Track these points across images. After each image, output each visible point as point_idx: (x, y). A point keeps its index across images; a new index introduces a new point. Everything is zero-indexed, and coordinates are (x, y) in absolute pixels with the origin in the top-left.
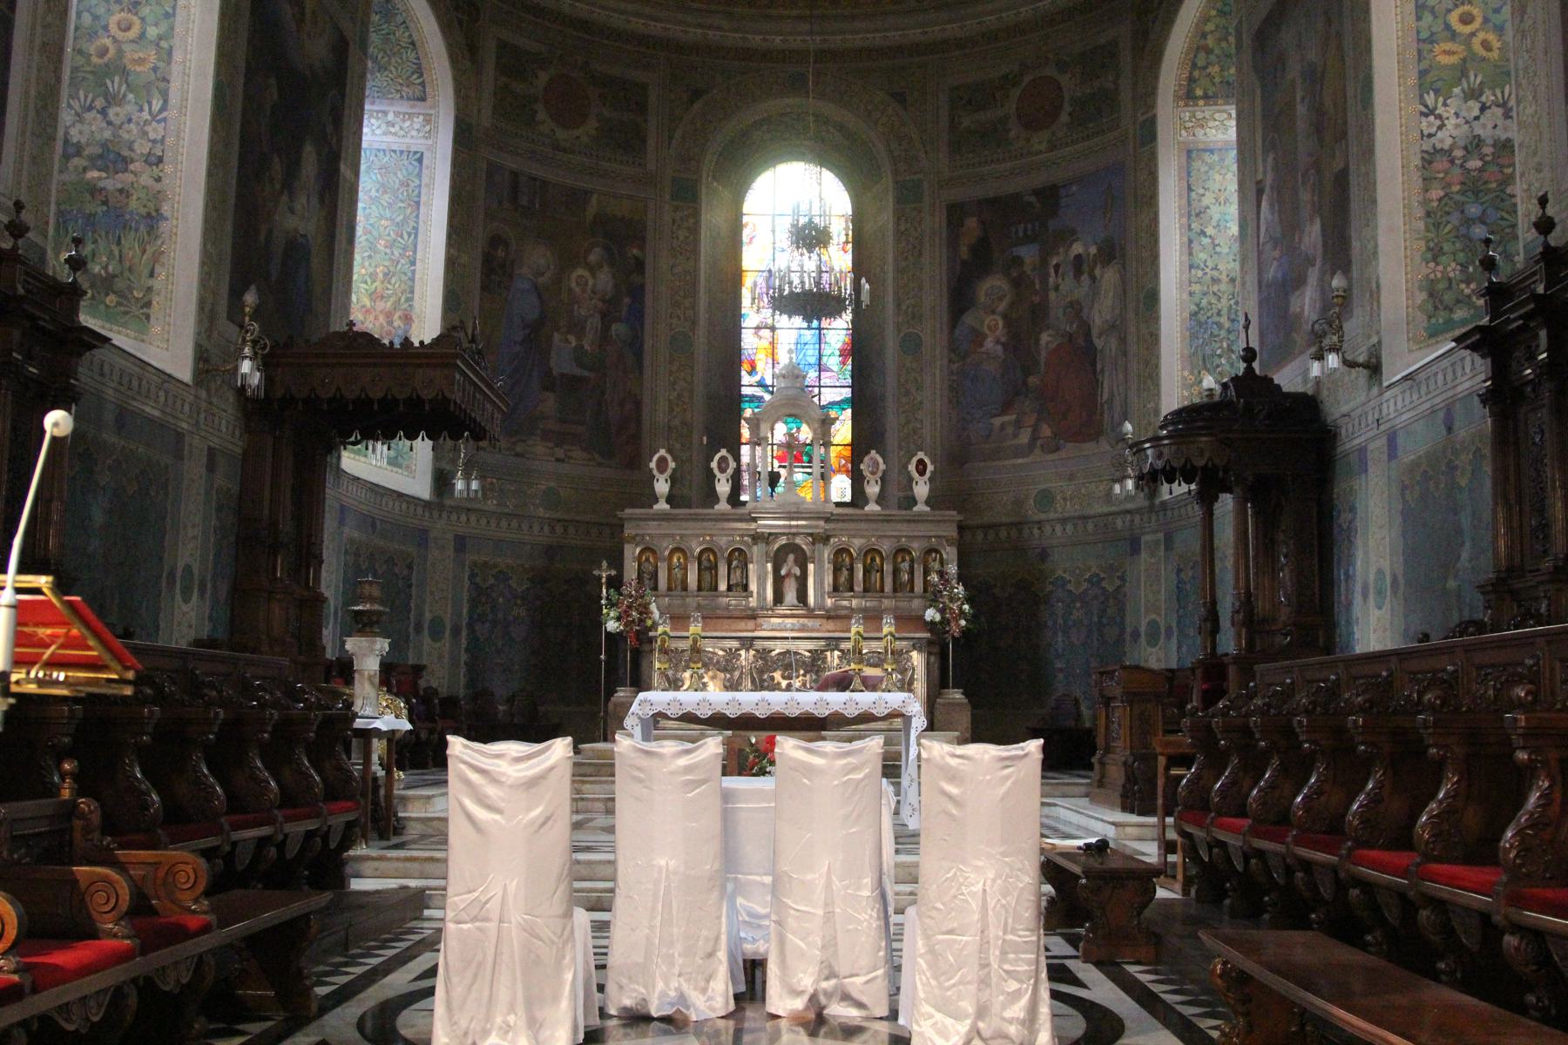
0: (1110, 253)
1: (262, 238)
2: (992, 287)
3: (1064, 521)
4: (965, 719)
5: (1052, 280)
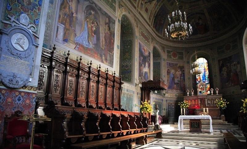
0: (239, 63)
1: (142, 72)
2: (224, 69)
3: (236, 95)
4: (224, 118)
5: (232, 67)
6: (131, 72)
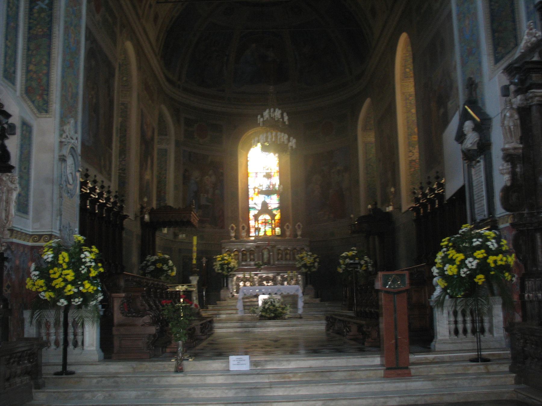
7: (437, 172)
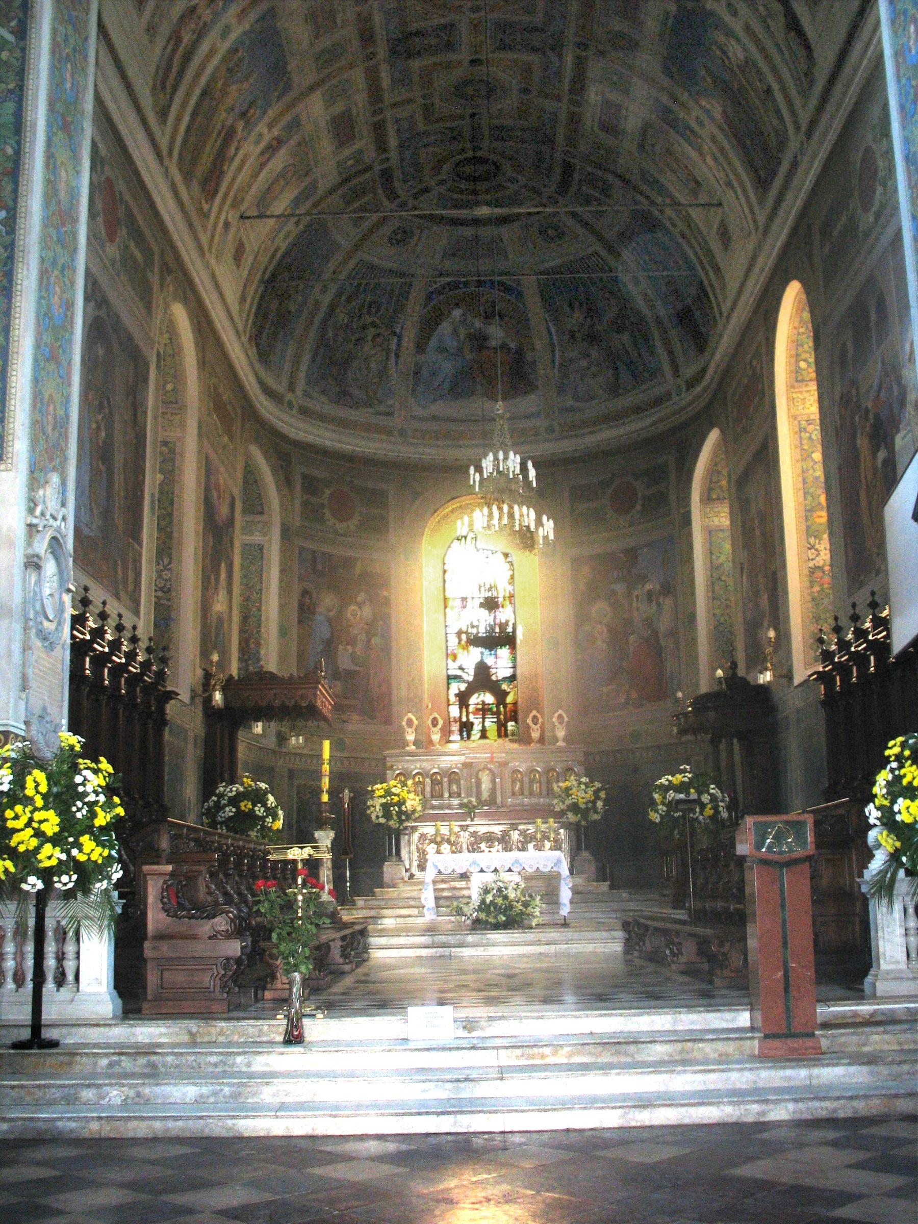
0: (667, 589)
5: (635, 604)
6: (167, 626)
7: (873, 593)
